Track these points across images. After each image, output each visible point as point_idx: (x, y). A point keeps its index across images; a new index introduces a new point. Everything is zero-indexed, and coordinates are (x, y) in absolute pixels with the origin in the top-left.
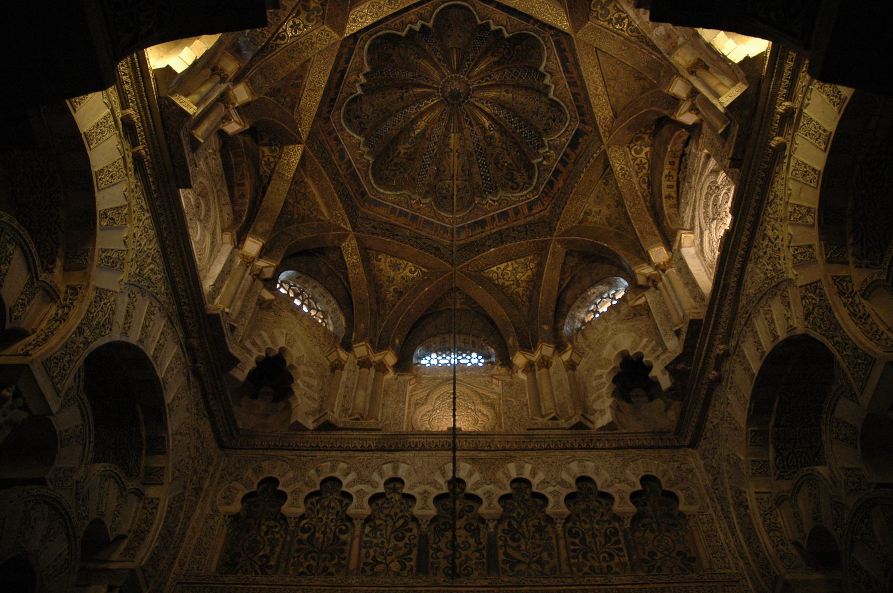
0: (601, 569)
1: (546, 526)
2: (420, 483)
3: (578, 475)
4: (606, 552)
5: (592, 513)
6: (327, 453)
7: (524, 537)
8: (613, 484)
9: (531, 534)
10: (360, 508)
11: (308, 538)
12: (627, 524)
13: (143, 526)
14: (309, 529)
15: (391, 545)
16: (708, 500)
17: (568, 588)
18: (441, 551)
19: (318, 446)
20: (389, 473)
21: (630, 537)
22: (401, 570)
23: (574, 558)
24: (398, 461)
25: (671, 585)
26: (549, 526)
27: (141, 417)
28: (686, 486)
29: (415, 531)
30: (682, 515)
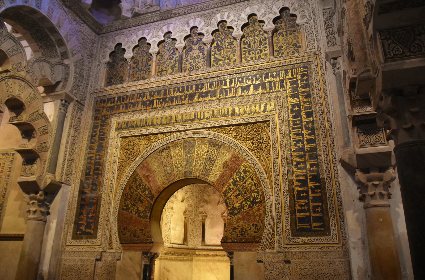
0: (256, 58)
1: (233, 42)
2: (178, 32)
3: (249, 14)
4: (259, 50)
5: (255, 32)
6: (140, 27)
7: (223, 49)
8: (265, 15)
9: (226, 46)
10: (154, 49)
11: (136, 66)
12: (270, 34)
13: (67, 76)
14: (136, 62)
15: (168, 62)
16: (312, 16)
17: (238, 69)
18: (188, 61)
19: (135, 24)
20: (166, 31)
21: (270, 41)
22: (172, 72)
23: (244, 54)
24: (169, 23)
25: (284, 61)
26: (235, 41)
27: (49, 33)
28: (303, 9)
29: (178, 55)
30: (298, 25)
